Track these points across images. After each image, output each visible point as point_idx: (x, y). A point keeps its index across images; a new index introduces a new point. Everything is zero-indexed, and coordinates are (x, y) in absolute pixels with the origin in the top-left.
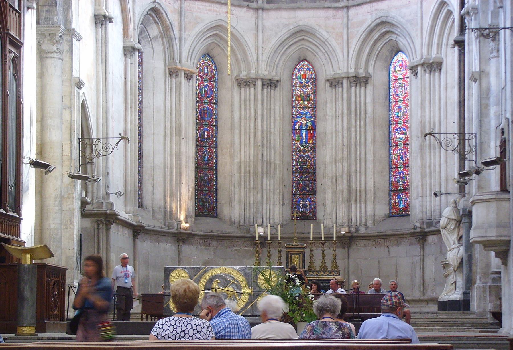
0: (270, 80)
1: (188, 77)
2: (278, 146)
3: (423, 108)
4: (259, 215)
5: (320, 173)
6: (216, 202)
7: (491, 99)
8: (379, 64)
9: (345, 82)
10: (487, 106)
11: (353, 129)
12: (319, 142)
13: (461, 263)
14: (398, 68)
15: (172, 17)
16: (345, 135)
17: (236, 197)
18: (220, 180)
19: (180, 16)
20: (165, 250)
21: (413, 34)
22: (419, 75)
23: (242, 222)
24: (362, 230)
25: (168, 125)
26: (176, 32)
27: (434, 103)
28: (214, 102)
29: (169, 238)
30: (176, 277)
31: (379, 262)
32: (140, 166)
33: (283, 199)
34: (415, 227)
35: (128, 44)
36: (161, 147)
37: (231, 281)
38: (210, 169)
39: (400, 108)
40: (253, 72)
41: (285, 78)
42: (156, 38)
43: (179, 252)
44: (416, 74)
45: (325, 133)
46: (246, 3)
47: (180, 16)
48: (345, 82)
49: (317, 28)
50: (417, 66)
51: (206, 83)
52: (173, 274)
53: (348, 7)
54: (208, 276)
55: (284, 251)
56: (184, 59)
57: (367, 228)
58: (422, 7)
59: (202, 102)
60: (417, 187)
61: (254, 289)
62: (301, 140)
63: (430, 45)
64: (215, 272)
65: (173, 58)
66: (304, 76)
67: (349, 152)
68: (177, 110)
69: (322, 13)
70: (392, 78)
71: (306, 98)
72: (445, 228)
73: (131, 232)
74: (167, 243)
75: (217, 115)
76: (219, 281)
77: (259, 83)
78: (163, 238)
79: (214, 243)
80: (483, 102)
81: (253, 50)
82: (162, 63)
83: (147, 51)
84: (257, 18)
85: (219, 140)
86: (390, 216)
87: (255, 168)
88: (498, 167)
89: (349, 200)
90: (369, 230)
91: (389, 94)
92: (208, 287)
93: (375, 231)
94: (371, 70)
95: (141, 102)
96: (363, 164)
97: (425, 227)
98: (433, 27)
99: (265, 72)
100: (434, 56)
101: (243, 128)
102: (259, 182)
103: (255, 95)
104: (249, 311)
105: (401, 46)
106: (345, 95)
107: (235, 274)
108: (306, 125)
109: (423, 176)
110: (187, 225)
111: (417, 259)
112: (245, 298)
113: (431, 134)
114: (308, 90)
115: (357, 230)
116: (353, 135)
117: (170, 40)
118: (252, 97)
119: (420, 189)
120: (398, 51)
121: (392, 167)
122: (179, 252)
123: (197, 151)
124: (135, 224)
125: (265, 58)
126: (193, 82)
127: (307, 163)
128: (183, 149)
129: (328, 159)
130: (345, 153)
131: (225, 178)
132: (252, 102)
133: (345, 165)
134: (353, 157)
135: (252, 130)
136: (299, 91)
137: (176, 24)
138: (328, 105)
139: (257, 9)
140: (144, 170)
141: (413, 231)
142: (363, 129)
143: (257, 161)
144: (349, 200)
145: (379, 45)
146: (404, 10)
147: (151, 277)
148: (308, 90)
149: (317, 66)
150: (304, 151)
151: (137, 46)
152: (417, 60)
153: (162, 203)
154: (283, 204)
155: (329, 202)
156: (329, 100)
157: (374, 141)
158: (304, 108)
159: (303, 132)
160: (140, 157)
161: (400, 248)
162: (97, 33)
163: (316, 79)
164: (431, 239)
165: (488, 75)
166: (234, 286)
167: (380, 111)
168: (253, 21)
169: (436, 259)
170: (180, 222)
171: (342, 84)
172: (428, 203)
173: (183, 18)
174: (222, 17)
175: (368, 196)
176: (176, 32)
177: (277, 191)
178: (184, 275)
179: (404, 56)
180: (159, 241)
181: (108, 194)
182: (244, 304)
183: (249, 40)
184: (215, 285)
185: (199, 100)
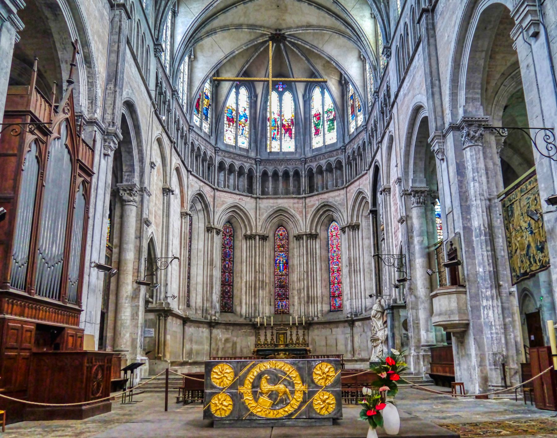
0: (263, 236)
1: (218, 233)
2: (267, 272)
3: (349, 250)
4: (257, 311)
5: (291, 287)
6: (232, 304)
7: (415, 233)
8: (322, 228)
9: (304, 237)
10: (412, 237)
11: (309, 263)
12: (290, 270)
13: (387, 339)
14: (333, 230)
15: (209, 200)
16: (305, 265)
17: (244, 301)
18: (235, 291)
19: (214, 199)
20: (203, 332)
21: (342, 210)
22: (347, 232)
23: (247, 315)
24: (316, 319)
25: (206, 259)
26: (212, 208)
27: (356, 247)
28: (232, 248)
29: (205, 326)
30: (219, 373)
31: (326, 338)
32: (189, 282)
33: (270, 302)
34: (348, 317)
35: (183, 211)
36: (202, 273)
37: (282, 378)
38: (229, 285)
39: (335, 251)
40: (254, 231)
41: (271, 235)
42: (200, 210)
43: (211, 333)
44: (344, 232)
45: (293, 265)
46: (250, 195)
47: (214, 199)
48: (304, 237)
49: (289, 208)
50: (345, 227)
51: (228, 237)
52: (215, 370)
53: (305, 198)
54: (255, 372)
55: (275, 332)
56: (216, 223)
58: (347, 196)
59: (225, 248)
60: (347, 294)
61: (309, 386)
62: (280, 269)
63: (352, 216)
64: (264, 368)
65: (209, 222)
66: (281, 235)
67: (308, 275)
68: (211, 251)
69: (292, 201)
70: (330, 235)
71: (283, 246)
72: (374, 317)
73: (182, 322)
74: (204, 328)
75: (233, 255)
76: (268, 378)
77: (257, 237)
78: (201, 325)
79: (231, 328)
80: (409, 234)
81: (254, 220)
82: (203, 224)
83: (195, 218)
84: (256, 203)
85: (234, 269)
86: (330, 311)
87: (255, 284)
89: (308, 302)
90: (319, 319)
91: (328, 244)
92: (255, 384)
93: (322, 319)
94: (318, 231)
95: (190, 246)
96: (315, 282)
97: (353, 316)
98: (354, 206)
99: (260, 231)
100: (354, 222)
101: (248, 262)
102: (257, 293)
103: (255, 244)
104: (305, 413)
105: (335, 218)
106: (305, 244)
107: (287, 369)
108: (283, 261)
109: (351, 288)
111: (348, 336)
112: (299, 396)
114: (283, 242)
115: (313, 319)
116: (309, 266)
118: (253, 245)
119: (349, 295)
120: (332, 220)
121: (331, 283)
122: (211, 333)
123: (222, 275)
124: (184, 316)
125: (261, 224)
126: (220, 236)
127: (283, 281)
128: (214, 273)
129: (295, 280)
130: (305, 276)
131: (238, 290)
132: (253, 248)
133: (305, 282)
134: (310, 278)
135: (253, 263)
136: (279, 243)
137: (212, 204)
138: (295, 250)
139: (256, 198)
140: (191, 285)
141: (346, 319)
142: (315, 263)
143: (256, 281)
144: (308, 302)
145: (323, 218)
146: (337, 198)
147: (194, 349)
148: (283, 242)
149: (288, 229)
150: (281, 275)
151: (189, 212)
152: (344, 224)
153: (201, 305)
154: (270, 305)
155: (296, 303)
156: (295, 247)
157: (321, 270)
158: (281, 252)
159: (281, 265)
160: (189, 278)
161: (338, 329)
162: (164, 199)
163: (288, 236)
164: (357, 323)
165: (411, 218)
166: (286, 383)
167: (324, 253)
168: (254, 204)
169: (361, 335)
171: (303, 238)
172: (354, 303)
173: (216, 200)
174: (237, 201)
175: (319, 300)
176: (212, 208)
177: (267, 298)
178: (228, 371)
179: (336, 224)
180: (199, 327)
181: (166, 297)
182: (298, 404)
183: (252, 214)
184: (264, 382)
185: (224, 246)
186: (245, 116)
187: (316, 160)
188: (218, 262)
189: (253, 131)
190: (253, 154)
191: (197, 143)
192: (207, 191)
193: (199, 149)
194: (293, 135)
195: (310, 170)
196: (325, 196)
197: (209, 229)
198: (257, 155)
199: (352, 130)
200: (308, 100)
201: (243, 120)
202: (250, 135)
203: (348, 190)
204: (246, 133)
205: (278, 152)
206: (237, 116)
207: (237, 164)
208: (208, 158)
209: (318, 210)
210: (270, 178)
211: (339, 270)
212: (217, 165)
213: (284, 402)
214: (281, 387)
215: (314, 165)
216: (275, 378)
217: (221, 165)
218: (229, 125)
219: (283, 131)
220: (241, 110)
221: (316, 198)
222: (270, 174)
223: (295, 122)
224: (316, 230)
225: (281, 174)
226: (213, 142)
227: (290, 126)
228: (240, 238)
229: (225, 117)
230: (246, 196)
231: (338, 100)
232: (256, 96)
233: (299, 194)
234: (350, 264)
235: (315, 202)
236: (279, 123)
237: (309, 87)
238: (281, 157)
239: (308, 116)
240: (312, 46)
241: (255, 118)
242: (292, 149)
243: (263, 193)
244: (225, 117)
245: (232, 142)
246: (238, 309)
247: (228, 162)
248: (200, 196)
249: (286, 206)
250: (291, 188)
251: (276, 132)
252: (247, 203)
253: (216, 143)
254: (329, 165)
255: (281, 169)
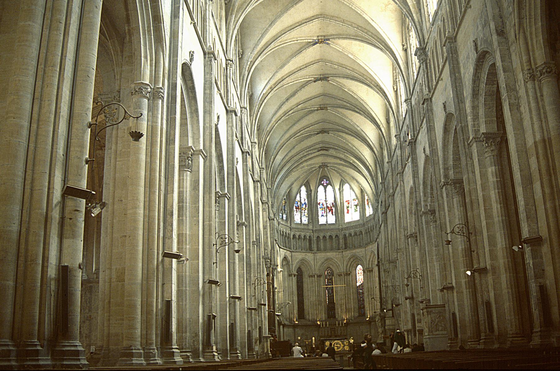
1: (294, 276)
3: (368, 284)
15: (289, 258)
28: (302, 282)
57: (352, 320)
63: (369, 265)
69: (335, 254)
77: (316, 276)
86: (359, 316)
88: (391, 312)
99: (318, 273)
110: (297, 322)
112: (342, 347)
113: (373, 298)
114: (331, 277)
115: (349, 321)
117: (289, 265)
121: (359, 301)
126: (296, 277)
148: (331, 277)
153: (288, 316)
157: (353, 293)
164: (373, 323)
170: (294, 321)
183: (312, 262)
185: (298, 282)
186: (305, 203)
187: (348, 230)
188: (295, 292)
189: (310, 212)
190: (311, 227)
191: (282, 229)
192: (288, 254)
193: (283, 232)
194: (334, 213)
195: (345, 235)
196: (354, 251)
197: (290, 275)
198: (313, 227)
199: (367, 215)
200: (341, 191)
201: (304, 206)
202: (309, 215)
203: (366, 249)
204: (306, 214)
205: (325, 224)
206: (300, 205)
207: (303, 234)
208: (287, 235)
209: (350, 259)
210: (322, 241)
211: (363, 293)
212: (292, 237)
213: (339, 348)
214: (338, 345)
215: (347, 233)
216: (337, 344)
217: (294, 236)
218: (297, 211)
219: (328, 211)
220: (303, 202)
221: (348, 252)
222: (321, 238)
223: (335, 204)
224: (349, 270)
225: (328, 238)
226: (289, 225)
227: (331, 207)
228: (306, 277)
229: (294, 207)
230: (309, 253)
231: (359, 195)
232: (311, 191)
233: (339, 249)
234: (369, 291)
235: (348, 253)
236: (325, 206)
237: (342, 183)
238: (327, 227)
239: (342, 201)
240: (344, 171)
241: (311, 204)
242: (334, 222)
243: (318, 250)
244: (294, 207)
245: (299, 222)
246: (307, 317)
247: (297, 234)
248: (285, 258)
249: (331, 257)
250: (334, 245)
251: (323, 212)
252: (309, 256)
253: (291, 225)
254: (356, 234)
255: (328, 234)
